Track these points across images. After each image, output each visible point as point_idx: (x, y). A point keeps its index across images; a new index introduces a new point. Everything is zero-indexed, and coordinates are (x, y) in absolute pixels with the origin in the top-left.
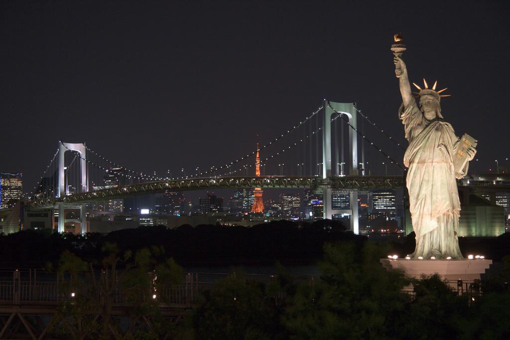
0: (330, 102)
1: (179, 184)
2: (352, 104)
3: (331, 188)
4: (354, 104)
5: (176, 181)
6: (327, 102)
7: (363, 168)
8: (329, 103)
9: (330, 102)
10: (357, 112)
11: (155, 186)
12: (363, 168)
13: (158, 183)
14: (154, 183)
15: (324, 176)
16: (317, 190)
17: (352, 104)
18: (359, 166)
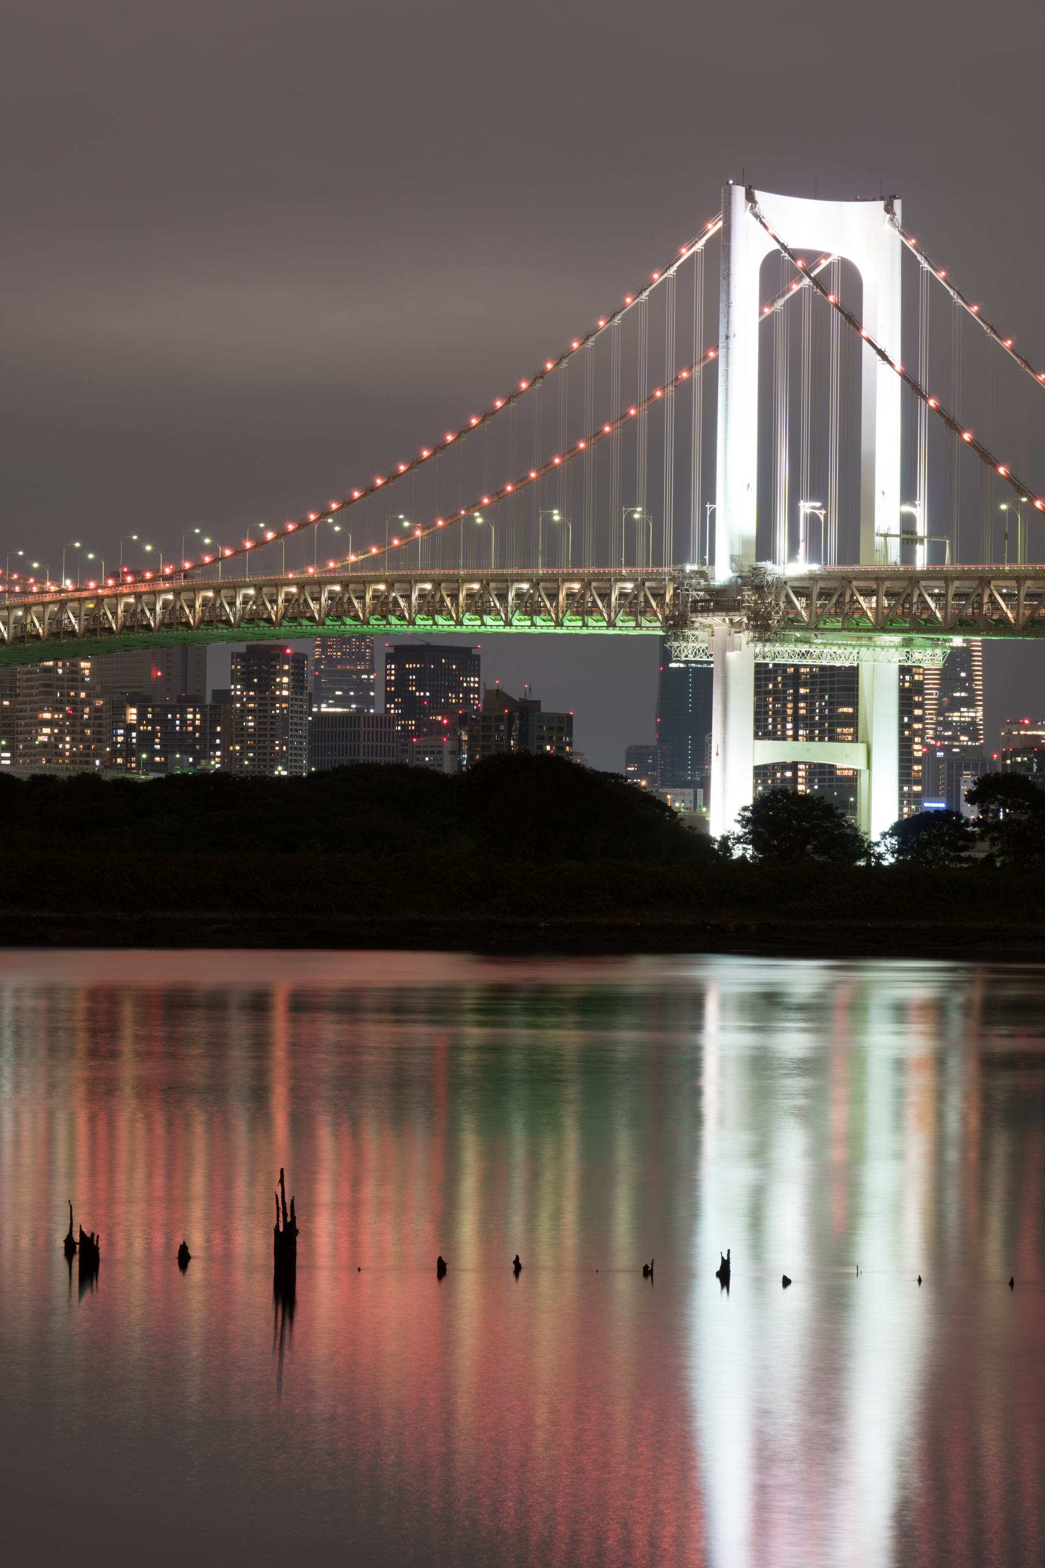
0: (759, 195)
1: (114, 614)
2: (880, 205)
3: (748, 629)
4: (889, 209)
5: (99, 600)
6: (739, 193)
7: (921, 529)
8: (750, 197)
9: (759, 195)
10: (904, 248)
11: (17, 620)
12: (921, 529)
13: (27, 608)
14: (10, 608)
15: (722, 574)
16: (686, 639)
17: (880, 205)
18: (907, 523)
